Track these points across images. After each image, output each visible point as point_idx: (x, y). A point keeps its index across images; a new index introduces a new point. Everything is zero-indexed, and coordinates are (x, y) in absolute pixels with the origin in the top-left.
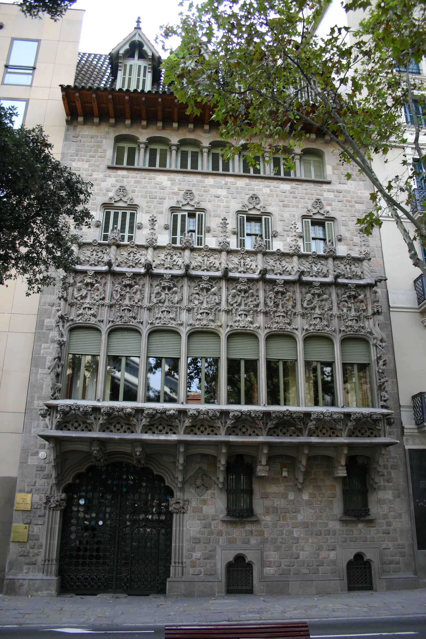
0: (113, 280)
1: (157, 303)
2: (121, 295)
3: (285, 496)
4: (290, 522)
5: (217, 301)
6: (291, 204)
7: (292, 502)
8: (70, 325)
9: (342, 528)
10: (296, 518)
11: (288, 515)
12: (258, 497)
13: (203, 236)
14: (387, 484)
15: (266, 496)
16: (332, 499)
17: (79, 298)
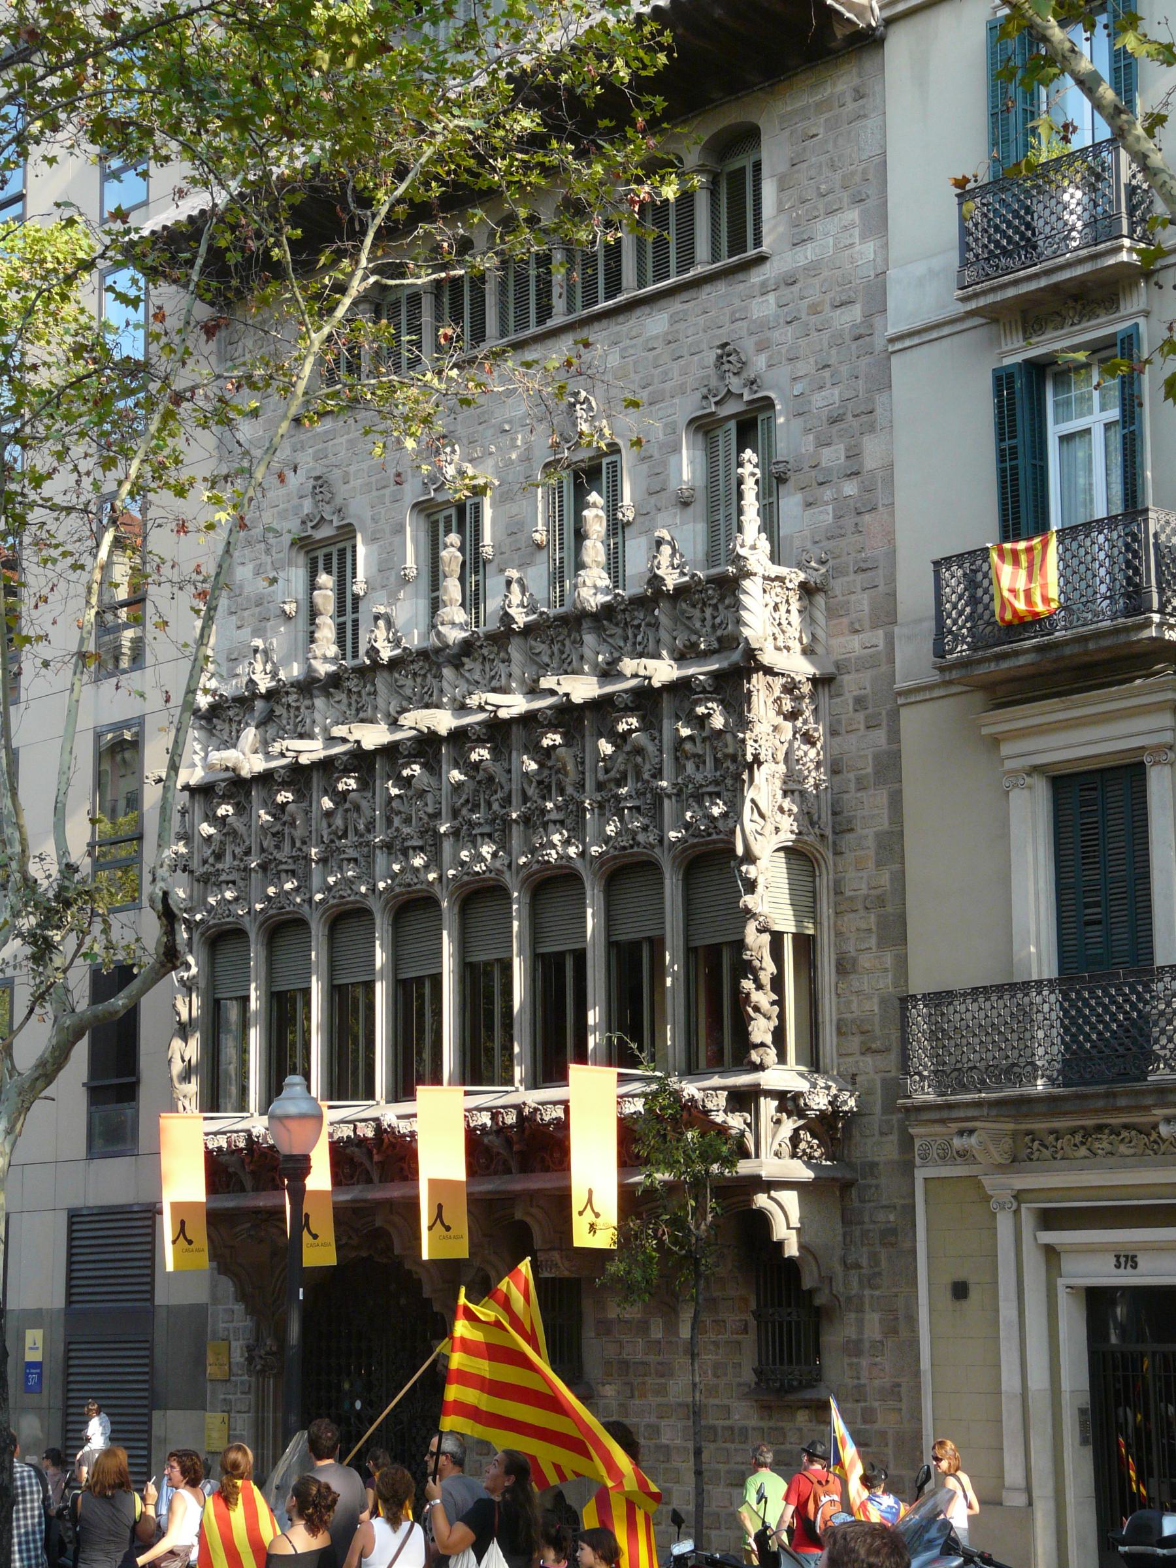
0: (264, 794)
1: (332, 841)
2: (274, 835)
3: (643, 1327)
4: (653, 1400)
5: (430, 810)
6: (669, 384)
7: (655, 1346)
8: (202, 934)
9: (763, 1424)
10: (662, 1391)
11: (649, 1380)
12: (593, 1334)
13: (480, 577)
14: (867, 1292)
15: (605, 1328)
16: (740, 1337)
17: (211, 860)
